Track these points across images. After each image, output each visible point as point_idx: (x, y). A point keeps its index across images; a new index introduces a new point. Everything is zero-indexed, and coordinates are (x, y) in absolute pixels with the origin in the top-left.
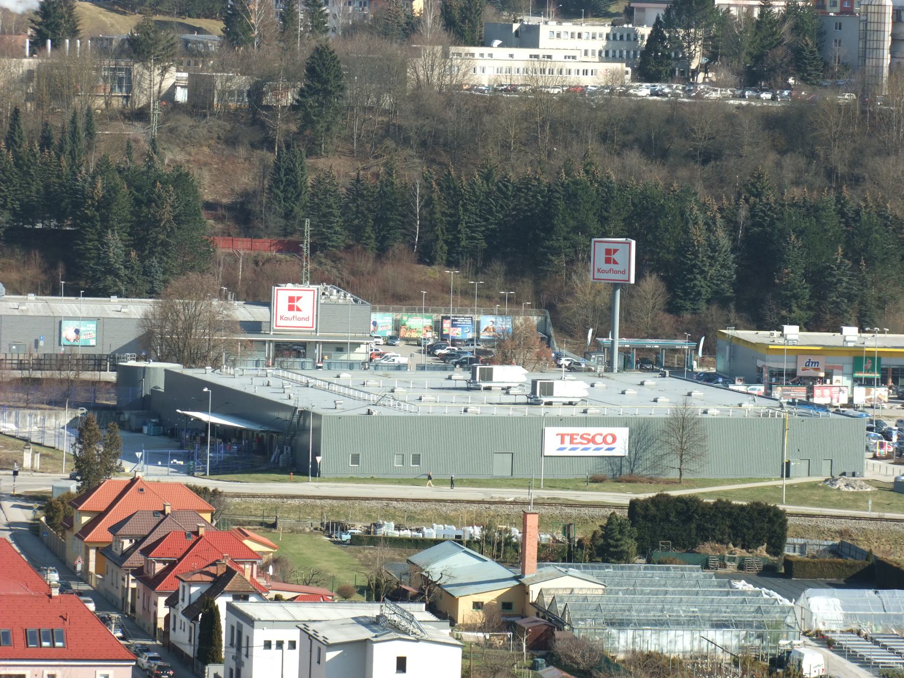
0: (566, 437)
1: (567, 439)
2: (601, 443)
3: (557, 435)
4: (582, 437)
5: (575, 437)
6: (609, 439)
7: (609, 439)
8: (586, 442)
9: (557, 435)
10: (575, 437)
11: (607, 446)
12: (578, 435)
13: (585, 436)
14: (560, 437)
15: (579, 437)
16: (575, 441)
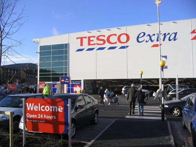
0: (83, 39)
1: (85, 41)
2: (116, 43)
3: (77, 38)
4: (98, 39)
5: (91, 39)
6: (123, 39)
7: (123, 39)
8: (102, 42)
9: (77, 38)
10: (91, 39)
11: (119, 45)
12: (94, 37)
13: (100, 38)
14: (80, 39)
15: (95, 39)
16: (91, 43)
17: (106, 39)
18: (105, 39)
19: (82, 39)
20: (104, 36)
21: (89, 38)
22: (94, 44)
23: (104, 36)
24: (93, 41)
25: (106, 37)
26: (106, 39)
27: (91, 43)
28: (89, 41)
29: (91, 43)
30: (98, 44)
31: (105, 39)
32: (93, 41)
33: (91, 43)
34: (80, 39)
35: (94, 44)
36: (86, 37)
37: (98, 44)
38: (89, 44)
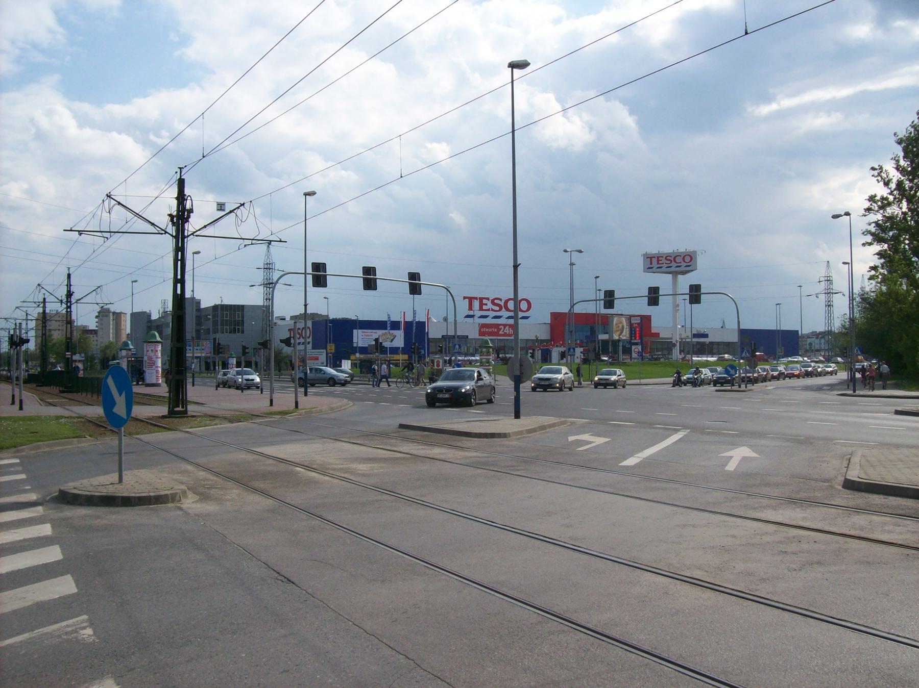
1: (476, 304)
3: (465, 298)
4: (493, 302)
5: (485, 301)
12: (488, 299)
13: (496, 301)
14: (468, 300)
15: (489, 303)
17: (503, 305)
18: (502, 304)
19: (471, 300)
20: (501, 300)
21: (481, 299)
22: (488, 310)
23: (501, 300)
24: (486, 304)
25: (503, 301)
26: (503, 305)
27: (485, 307)
28: (481, 304)
29: (484, 308)
30: (493, 310)
31: (502, 304)
32: (486, 304)
33: (484, 308)
34: (468, 300)
35: (488, 310)
36: (476, 298)
37: (493, 310)
38: (481, 309)
